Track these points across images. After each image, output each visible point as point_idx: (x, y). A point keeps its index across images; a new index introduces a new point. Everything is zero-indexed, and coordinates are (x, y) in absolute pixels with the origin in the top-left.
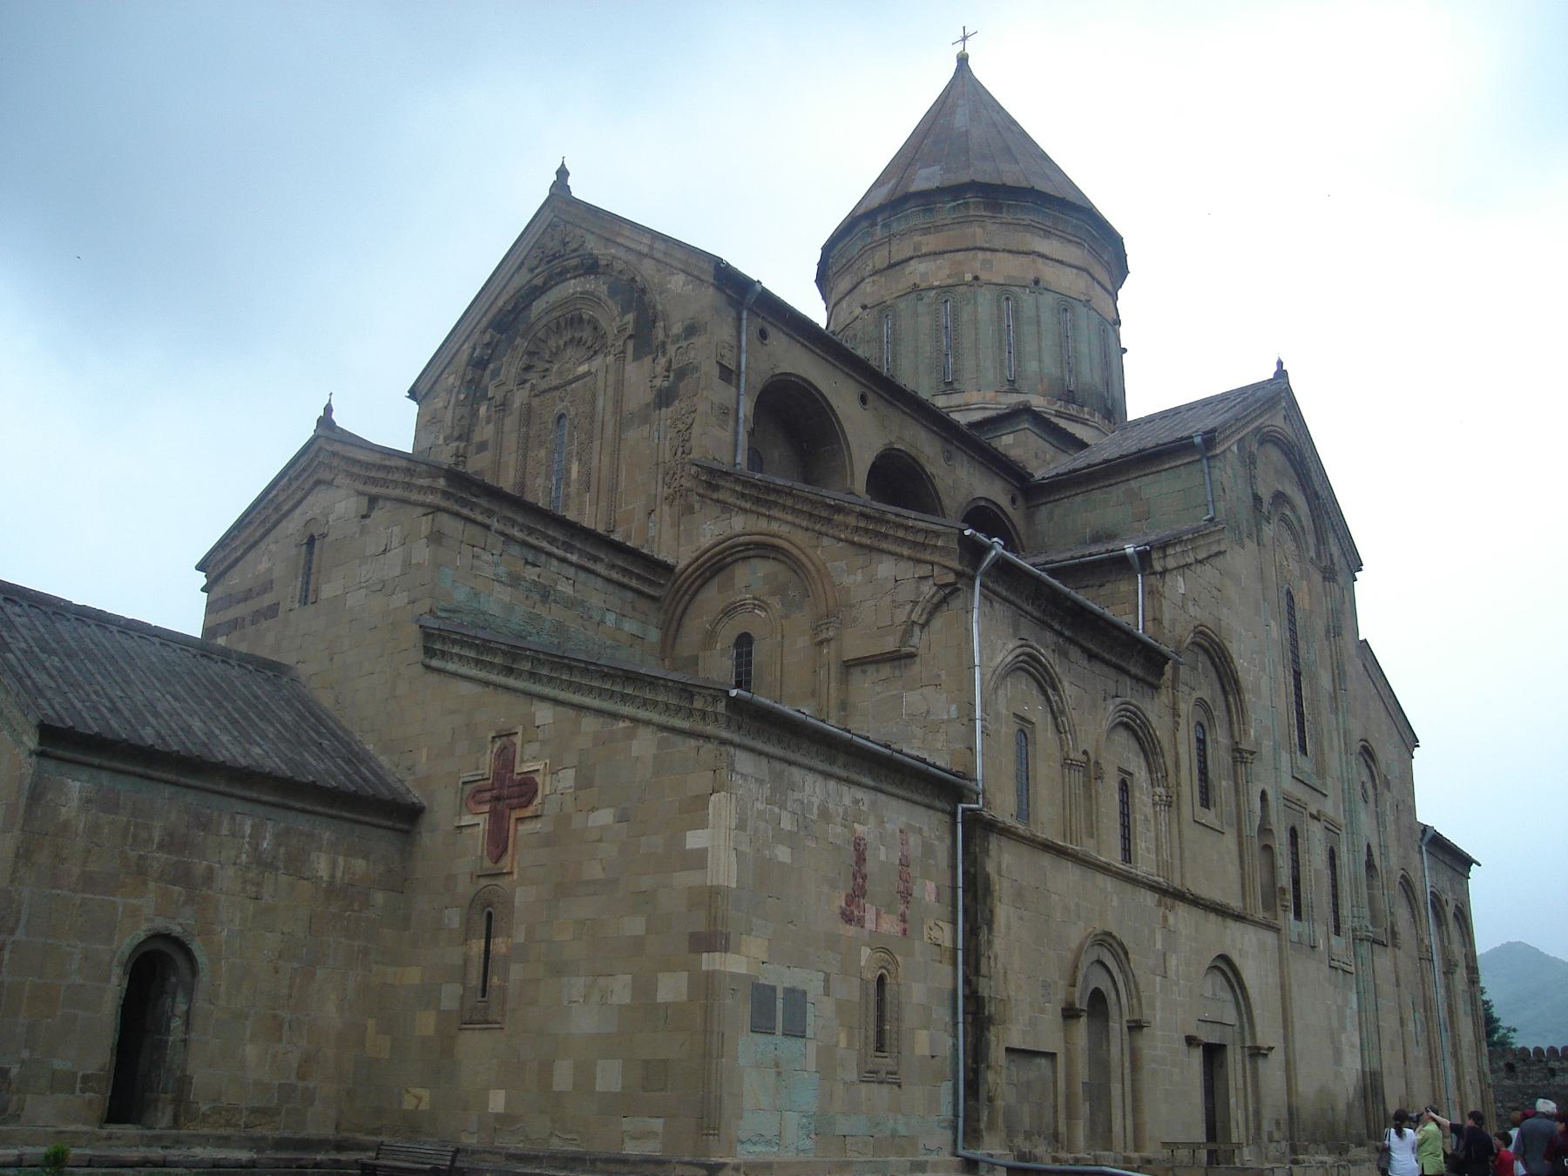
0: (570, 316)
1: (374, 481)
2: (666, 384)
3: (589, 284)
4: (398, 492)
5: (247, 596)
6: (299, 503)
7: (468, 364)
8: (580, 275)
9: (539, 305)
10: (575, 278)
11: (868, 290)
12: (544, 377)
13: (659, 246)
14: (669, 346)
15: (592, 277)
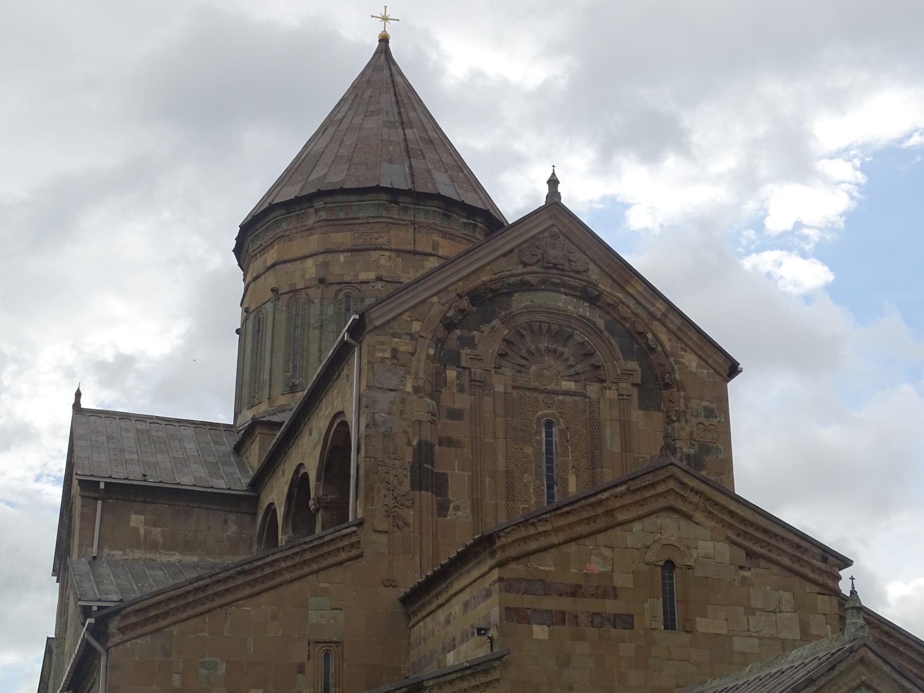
0: (558, 328)
1: (752, 538)
2: (692, 451)
3: (585, 310)
4: (786, 561)
5: (575, 592)
6: (639, 518)
7: (441, 322)
8: (575, 296)
9: (521, 301)
10: (566, 294)
11: (383, 261)
12: (520, 371)
13: (678, 322)
14: (688, 417)
15: (586, 304)
